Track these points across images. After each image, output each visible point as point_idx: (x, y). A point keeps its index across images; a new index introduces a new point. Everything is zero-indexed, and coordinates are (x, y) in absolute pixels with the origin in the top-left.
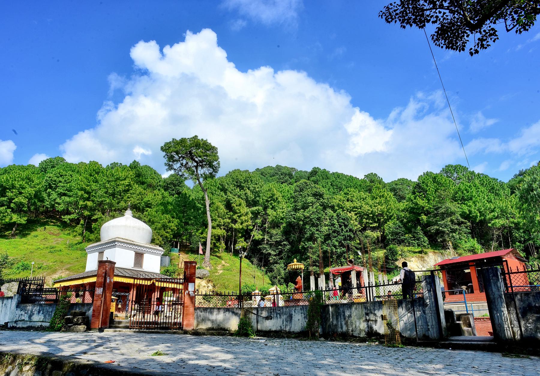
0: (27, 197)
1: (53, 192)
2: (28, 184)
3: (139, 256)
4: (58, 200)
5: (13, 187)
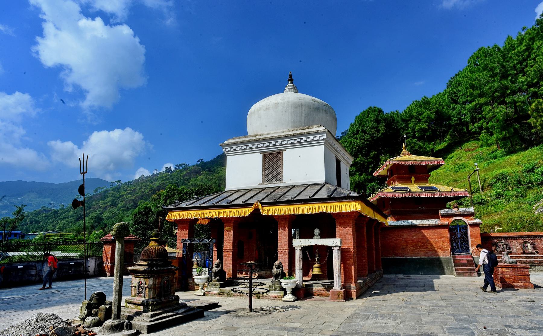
0: (426, 122)
1: (458, 105)
2: (426, 109)
3: (272, 162)
4: (463, 112)
5: (412, 117)
